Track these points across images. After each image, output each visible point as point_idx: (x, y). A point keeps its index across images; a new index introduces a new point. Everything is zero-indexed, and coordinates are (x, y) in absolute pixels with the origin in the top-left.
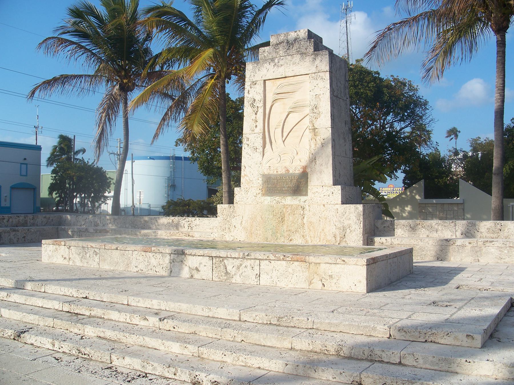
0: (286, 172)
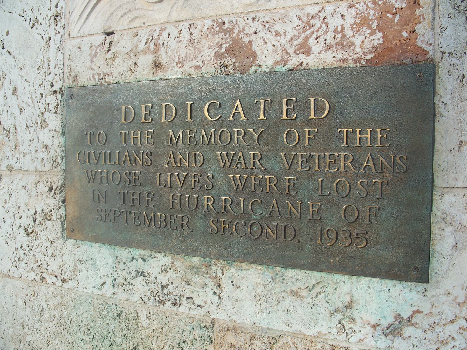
0: (228, 60)
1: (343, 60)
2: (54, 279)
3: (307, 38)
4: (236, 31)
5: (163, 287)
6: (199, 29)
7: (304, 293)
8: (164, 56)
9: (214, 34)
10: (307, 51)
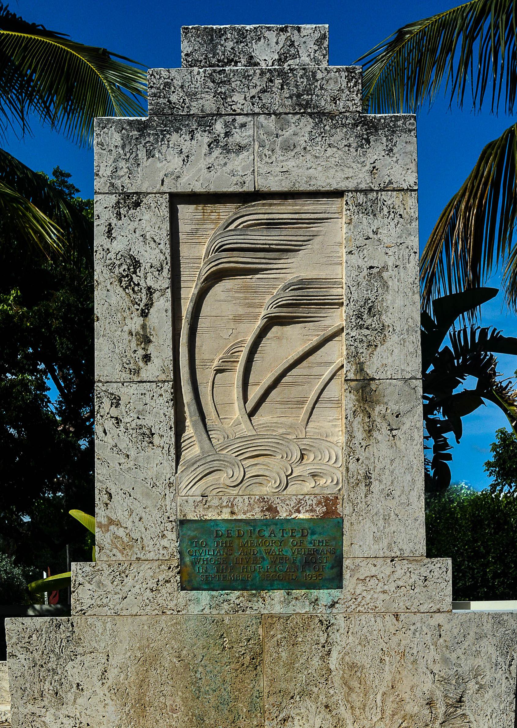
1: (312, 516)
2: (172, 612)
3: (299, 507)
4: (270, 502)
5: (237, 605)
6: (253, 500)
7: (300, 598)
8: (236, 509)
9: (260, 502)
10: (299, 512)
